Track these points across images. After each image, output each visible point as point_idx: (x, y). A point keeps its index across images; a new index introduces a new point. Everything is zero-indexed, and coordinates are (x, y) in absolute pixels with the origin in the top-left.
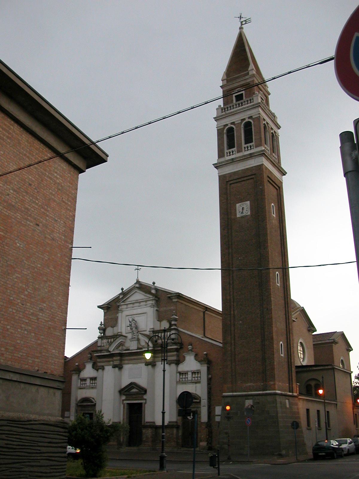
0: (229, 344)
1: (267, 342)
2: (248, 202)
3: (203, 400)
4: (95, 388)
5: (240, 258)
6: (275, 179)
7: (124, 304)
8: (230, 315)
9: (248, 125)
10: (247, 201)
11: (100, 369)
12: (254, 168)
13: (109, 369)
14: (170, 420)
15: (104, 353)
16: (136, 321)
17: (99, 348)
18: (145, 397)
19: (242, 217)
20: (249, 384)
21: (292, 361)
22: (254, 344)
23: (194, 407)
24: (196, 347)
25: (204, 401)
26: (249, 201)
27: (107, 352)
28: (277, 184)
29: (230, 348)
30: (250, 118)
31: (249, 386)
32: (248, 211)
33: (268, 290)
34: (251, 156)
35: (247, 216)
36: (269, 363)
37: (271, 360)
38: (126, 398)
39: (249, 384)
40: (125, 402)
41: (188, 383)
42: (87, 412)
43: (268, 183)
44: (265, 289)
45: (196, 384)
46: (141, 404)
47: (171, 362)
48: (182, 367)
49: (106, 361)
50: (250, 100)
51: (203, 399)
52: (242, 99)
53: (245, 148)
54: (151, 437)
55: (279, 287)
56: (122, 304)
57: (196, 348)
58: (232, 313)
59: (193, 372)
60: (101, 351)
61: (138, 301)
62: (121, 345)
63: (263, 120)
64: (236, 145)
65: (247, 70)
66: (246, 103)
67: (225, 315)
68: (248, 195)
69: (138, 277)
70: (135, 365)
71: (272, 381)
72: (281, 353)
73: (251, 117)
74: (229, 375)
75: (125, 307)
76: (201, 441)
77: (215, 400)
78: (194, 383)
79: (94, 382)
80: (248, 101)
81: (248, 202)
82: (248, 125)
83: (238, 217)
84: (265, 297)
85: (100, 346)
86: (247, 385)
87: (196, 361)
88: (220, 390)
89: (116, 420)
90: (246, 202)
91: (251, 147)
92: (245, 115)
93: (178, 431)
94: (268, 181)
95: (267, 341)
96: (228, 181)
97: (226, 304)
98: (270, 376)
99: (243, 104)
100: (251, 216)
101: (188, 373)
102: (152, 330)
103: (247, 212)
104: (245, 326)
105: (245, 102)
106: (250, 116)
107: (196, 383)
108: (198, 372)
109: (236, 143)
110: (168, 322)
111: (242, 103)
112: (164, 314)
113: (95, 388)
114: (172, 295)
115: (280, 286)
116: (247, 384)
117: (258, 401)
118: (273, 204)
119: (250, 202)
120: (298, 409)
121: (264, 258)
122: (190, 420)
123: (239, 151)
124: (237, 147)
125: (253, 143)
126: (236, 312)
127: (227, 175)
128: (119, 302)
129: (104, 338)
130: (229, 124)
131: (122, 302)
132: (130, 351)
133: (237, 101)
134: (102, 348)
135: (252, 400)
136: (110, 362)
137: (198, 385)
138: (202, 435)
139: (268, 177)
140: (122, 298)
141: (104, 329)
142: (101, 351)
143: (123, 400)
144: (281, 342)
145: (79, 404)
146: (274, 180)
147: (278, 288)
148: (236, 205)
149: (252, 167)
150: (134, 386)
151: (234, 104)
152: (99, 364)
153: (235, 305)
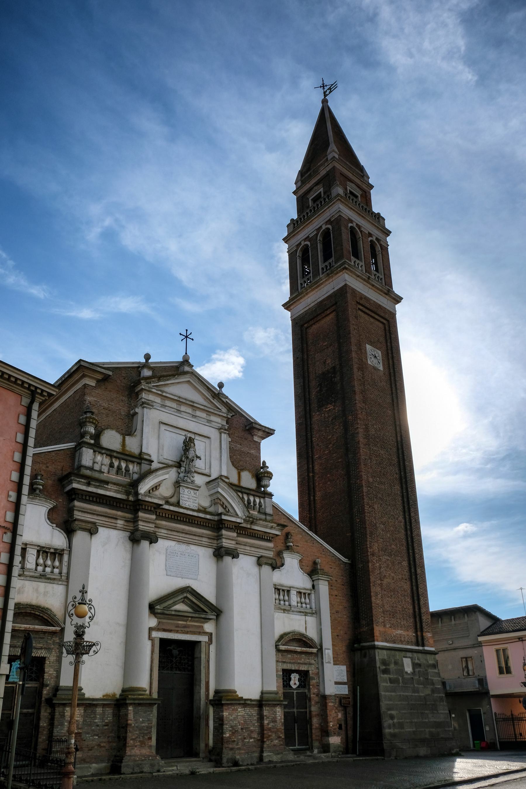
3: (326, 651)
15: (110, 490)
20: (399, 632)
24: (297, 545)
27: (116, 491)
31: (400, 634)
38: (159, 623)
40: (155, 634)
45: (305, 615)
57: (298, 546)
61: (195, 405)
69: (186, 353)
70: (183, 547)
78: (303, 614)
86: (397, 632)
88: (337, 636)
117: (419, 662)
122: (294, 689)
129: (103, 451)
132: (181, 510)
134: (96, 475)
136: (116, 519)
143: (151, 629)
150: (189, 596)
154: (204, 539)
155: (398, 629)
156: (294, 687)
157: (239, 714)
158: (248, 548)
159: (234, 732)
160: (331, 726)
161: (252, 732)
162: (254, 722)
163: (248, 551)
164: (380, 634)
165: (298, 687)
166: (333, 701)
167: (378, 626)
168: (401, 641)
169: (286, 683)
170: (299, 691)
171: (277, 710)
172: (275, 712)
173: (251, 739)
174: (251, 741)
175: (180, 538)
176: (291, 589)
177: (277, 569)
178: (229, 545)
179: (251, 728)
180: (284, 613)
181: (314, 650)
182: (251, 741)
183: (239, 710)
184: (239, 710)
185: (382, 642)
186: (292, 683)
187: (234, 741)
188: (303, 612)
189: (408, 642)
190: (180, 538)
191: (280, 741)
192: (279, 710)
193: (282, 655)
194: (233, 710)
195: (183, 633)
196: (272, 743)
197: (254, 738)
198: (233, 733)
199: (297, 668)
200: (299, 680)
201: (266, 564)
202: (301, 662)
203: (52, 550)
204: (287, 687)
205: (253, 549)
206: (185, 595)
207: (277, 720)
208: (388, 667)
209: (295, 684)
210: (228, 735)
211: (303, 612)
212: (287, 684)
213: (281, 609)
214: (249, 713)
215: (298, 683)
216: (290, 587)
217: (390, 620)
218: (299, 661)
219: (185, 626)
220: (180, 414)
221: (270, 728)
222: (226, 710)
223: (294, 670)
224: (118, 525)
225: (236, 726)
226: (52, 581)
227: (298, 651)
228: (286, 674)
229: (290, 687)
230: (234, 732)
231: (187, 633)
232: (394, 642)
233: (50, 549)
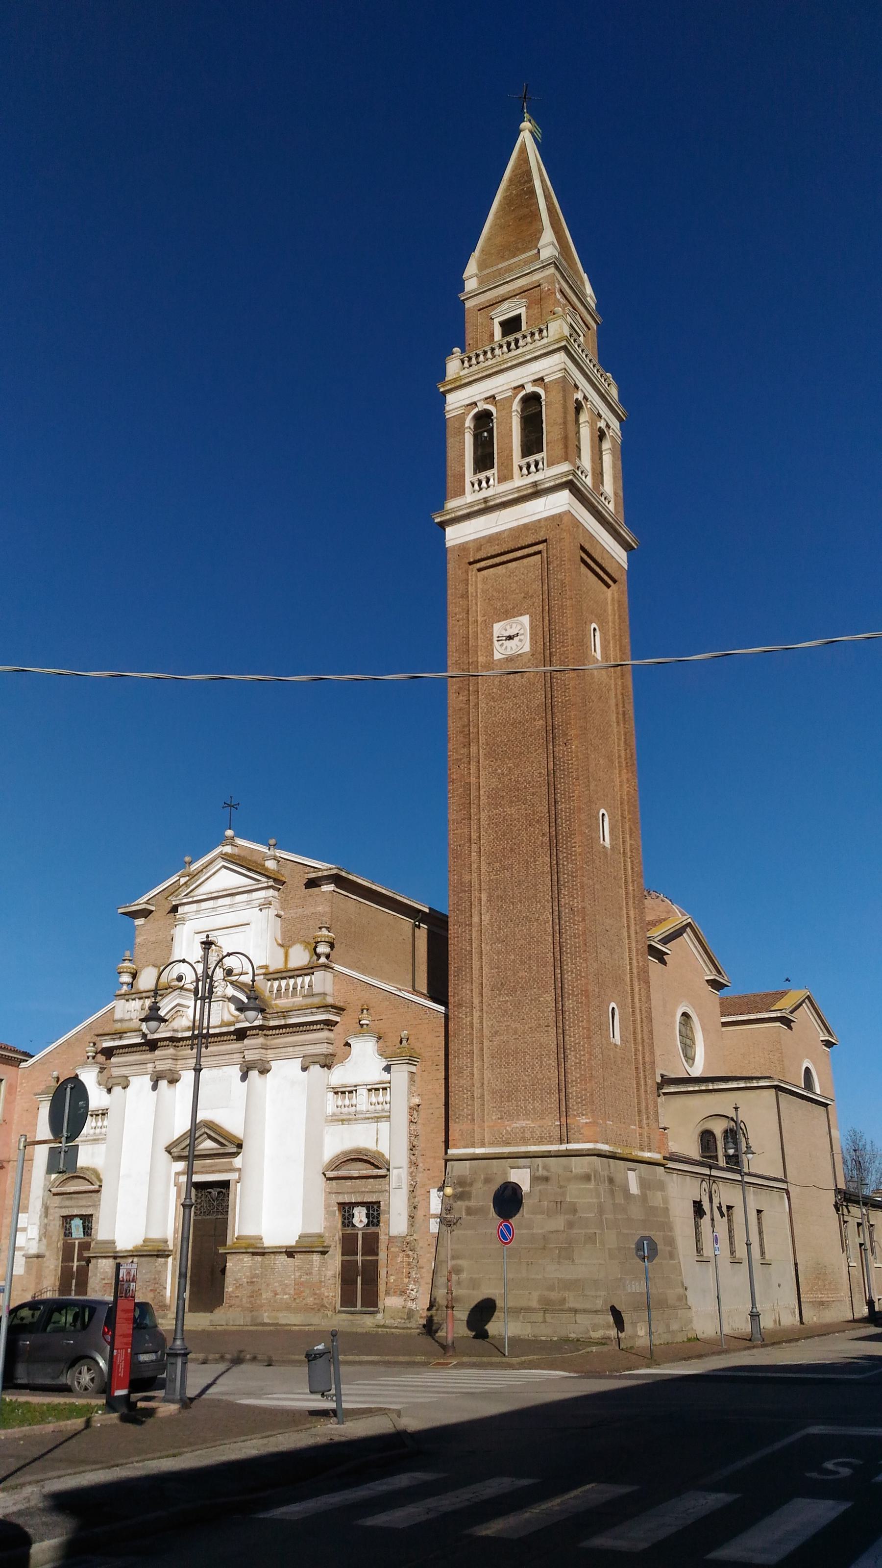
0: (466, 1007)
1: (570, 1001)
2: (525, 619)
4: (102, 1139)
5: (499, 771)
6: (603, 558)
7: (190, 900)
8: (471, 925)
9: (531, 401)
10: (521, 615)
11: (118, 1084)
12: (543, 523)
13: (141, 1083)
14: (304, 1232)
15: (129, 1038)
16: (221, 948)
17: (118, 1026)
18: (237, 1162)
19: (510, 659)
20: (523, 1123)
21: (647, 1059)
22: (535, 1007)
23: (373, 1192)
25: (399, 1175)
26: (528, 614)
28: (609, 570)
29: (468, 1019)
30: (540, 382)
31: (523, 1127)
32: (523, 642)
33: (573, 857)
34: (537, 492)
35: (520, 655)
36: (578, 1061)
37: (582, 1053)
39: (523, 1123)
41: (356, 1120)
42: (76, 1212)
43: (582, 565)
44: (565, 855)
46: (225, 1184)
47: (311, 1059)
48: (339, 1075)
49: (136, 1061)
50: (541, 331)
51: (395, 1168)
52: (518, 328)
53: (521, 468)
54: (247, 1282)
55: (609, 852)
56: (185, 901)
58: (475, 919)
59: (369, 1087)
60: (120, 1034)
62: (179, 1013)
63: (572, 388)
64: (496, 461)
65: (536, 247)
66: (529, 339)
67: (456, 927)
68: (525, 597)
71: (583, 1115)
72: (612, 1036)
73: (542, 379)
74: (465, 1096)
75: (194, 907)
76: (387, 1293)
77: (429, 1170)
78: (373, 1121)
79: (100, 1124)
80: (533, 334)
81: (525, 619)
82: (531, 401)
83: (495, 658)
84: (566, 876)
85: (121, 1021)
87: (380, 1057)
89: (155, 1235)
90: (520, 618)
91: (536, 465)
92: (524, 375)
93: (323, 1265)
94: (582, 559)
95: (569, 1000)
96: (472, 560)
97: (461, 895)
98: (579, 1100)
99: (519, 345)
100: (533, 655)
101: (356, 1091)
102: (263, 971)
103: (523, 645)
104: (513, 957)
105: (524, 337)
106: (536, 377)
107: (378, 1119)
108: (384, 1089)
109: (495, 456)
110: (306, 947)
111: (517, 341)
112: (299, 926)
113: (102, 1139)
114: (320, 874)
115: (613, 848)
116: (516, 1123)
117: (545, 1173)
118: (594, 625)
119: (531, 616)
120: (665, 1200)
121: (563, 770)
122: (359, 1229)
123: (502, 479)
124: (501, 464)
125: (544, 454)
126: (486, 918)
127: (471, 545)
128: (177, 896)
129: (134, 996)
130: (480, 400)
131: (184, 896)
133: (505, 334)
135: (528, 1170)
137: (384, 1126)
138: (391, 1275)
139: (582, 548)
140: (185, 883)
141: (132, 971)
142: (120, 1034)
144: (613, 1005)
145: (54, 1190)
146: (600, 561)
147: (606, 854)
148: (492, 626)
149: (539, 521)
151: (495, 346)
152: (116, 1072)
153: (484, 897)
154: (236, 1056)
155: (518, 1119)
156: (360, 1226)
157: (245, 1265)
158: (291, 1049)
159: (239, 1286)
160: (392, 1281)
161: (287, 1286)
162: (290, 1274)
163: (291, 1054)
164: (462, 1135)
165: (368, 1225)
166: (399, 1245)
167: (459, 1122)
168: (523, 1138)
169: (347, 1221)
170: (367, 1231)
171: (314, 1258)
172: (312, 1261)
173: (286, 1295)
174: (285, 1297)
175: (210, 1063)
176: (358, 1087)
177: (339, 1065)
178: (253, 1056)
179: (286, 1282)
180: (342, 1124)
181: (382, 1172)
182: (285, 1297)
183: (245, 1259)
184: (245, 1259)
185: (465, 1147)
186: (356, 1220)
187: (237, 1297)
188: (372, 1118)
189: (541, 1138)
190: (210, 1063)
191: (315, 1299)
192: (316, 1259)
193: (336, 1183)
194: (239, 1260)
195: (210, 1173)
196: (304, 1301)
197: (289, 1294)
198: (236, 1287)
199: (359, 1200)
200: (368, 1216)
201: (314, 1063)
202: (367, 1190)
203: (100, 1112)
204: (348, 1226)
205: (297, 1048)
206: (203, 1130)
207: (313, 1271)
208: (467, 1189)
209: (361, 1221)
210: (230, 1289)
211: (372, 1118)
212: (349, 1222)
213: (338, 1120)
214: (285, 1262)
215: (365, 1221)
216: (355, 1086)
217: (499, 1107)
218: (363, 1189)
219: (211, 1166)
220: (216, 911)
221: (303, 1281)
222: (230, 1260)
223: (355, 1203)
224: (148, 1070)
225: (239, 1279)
226: (97, 1142)
227: (354, 1176)
228: (346, 1209)
229: (354, 1226)
230: (239, 1286)
231: (213, 1172)
232: (507, 1143)
233: (98, 1110)
